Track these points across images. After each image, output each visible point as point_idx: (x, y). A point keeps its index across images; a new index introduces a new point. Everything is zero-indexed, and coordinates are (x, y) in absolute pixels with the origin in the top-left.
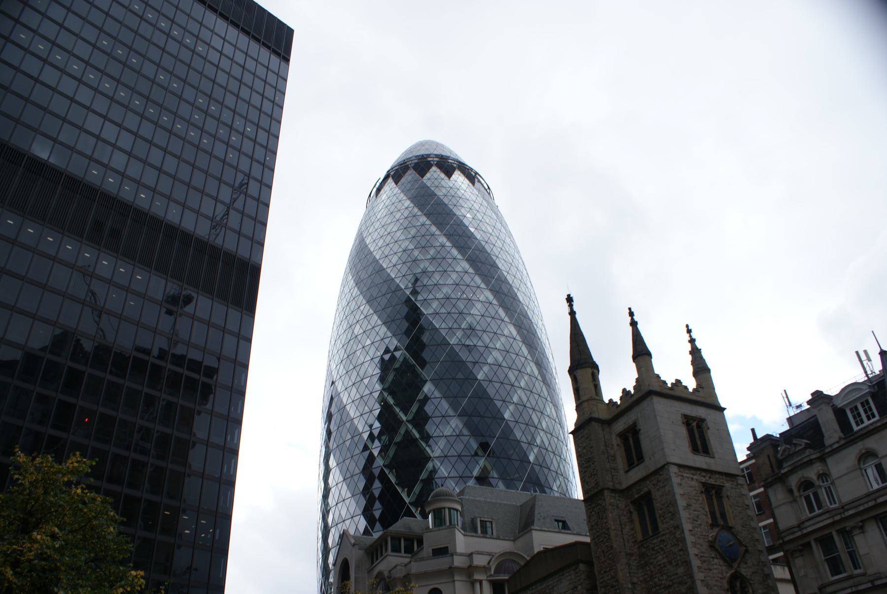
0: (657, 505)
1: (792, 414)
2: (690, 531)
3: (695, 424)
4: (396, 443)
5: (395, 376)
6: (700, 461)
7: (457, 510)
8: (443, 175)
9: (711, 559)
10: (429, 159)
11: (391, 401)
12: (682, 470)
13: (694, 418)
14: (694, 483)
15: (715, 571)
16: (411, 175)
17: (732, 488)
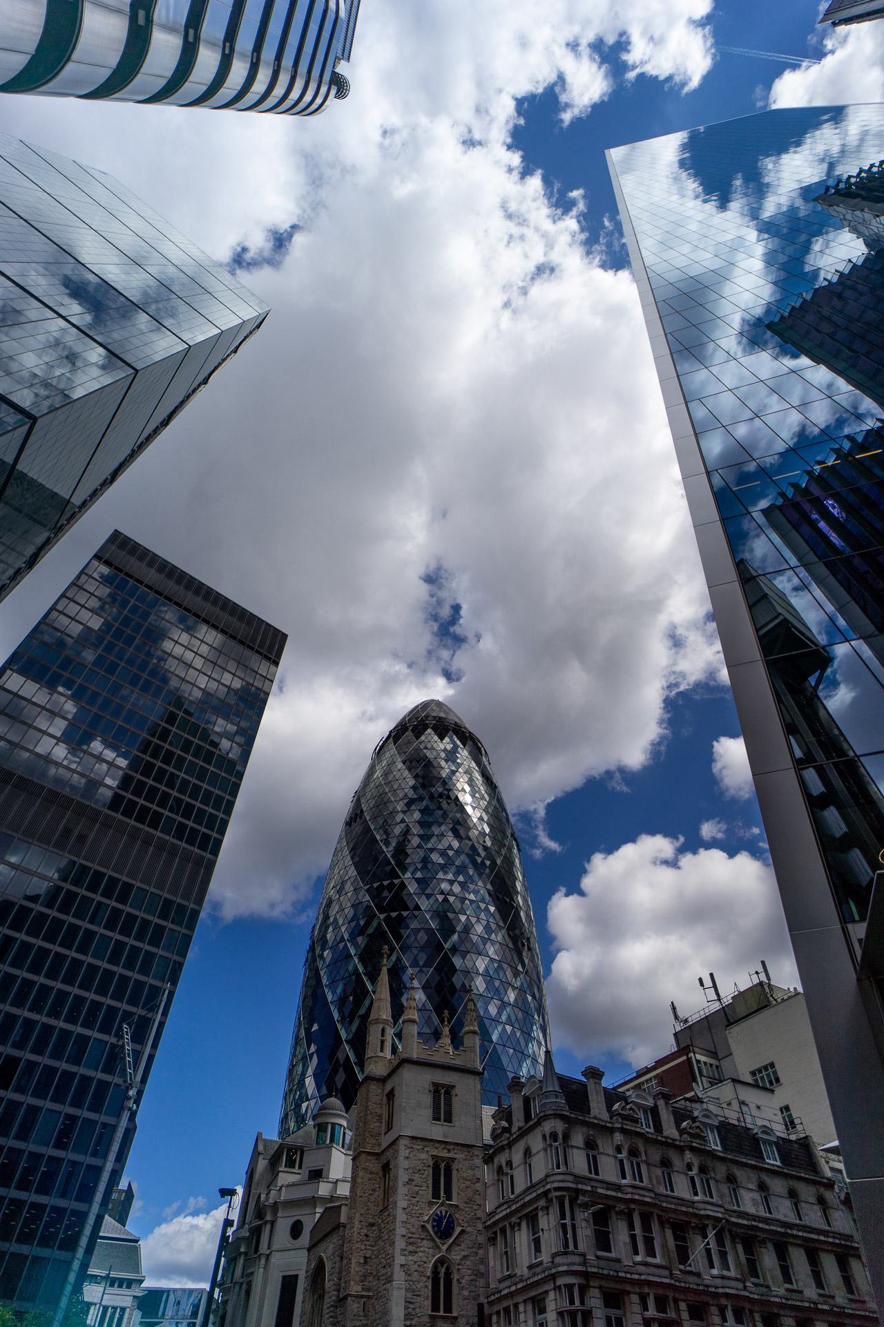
0: (391, 1175)
1: (678, 1029)
2: (404, 1209)
3: (443, 1091)
4: (359, 1016)
5: (368, 942)
6: (437, 1131)
7: (341, 1125)
8: (436, 738)
9: (419, 1241)
10: (427, 722)
11: (361, 969)
12: (414, 1141)
13: (443, 1086)
14: (424, 1156)
15: (421, 1254)
16: (409, 734)
17: (466, 1160)
